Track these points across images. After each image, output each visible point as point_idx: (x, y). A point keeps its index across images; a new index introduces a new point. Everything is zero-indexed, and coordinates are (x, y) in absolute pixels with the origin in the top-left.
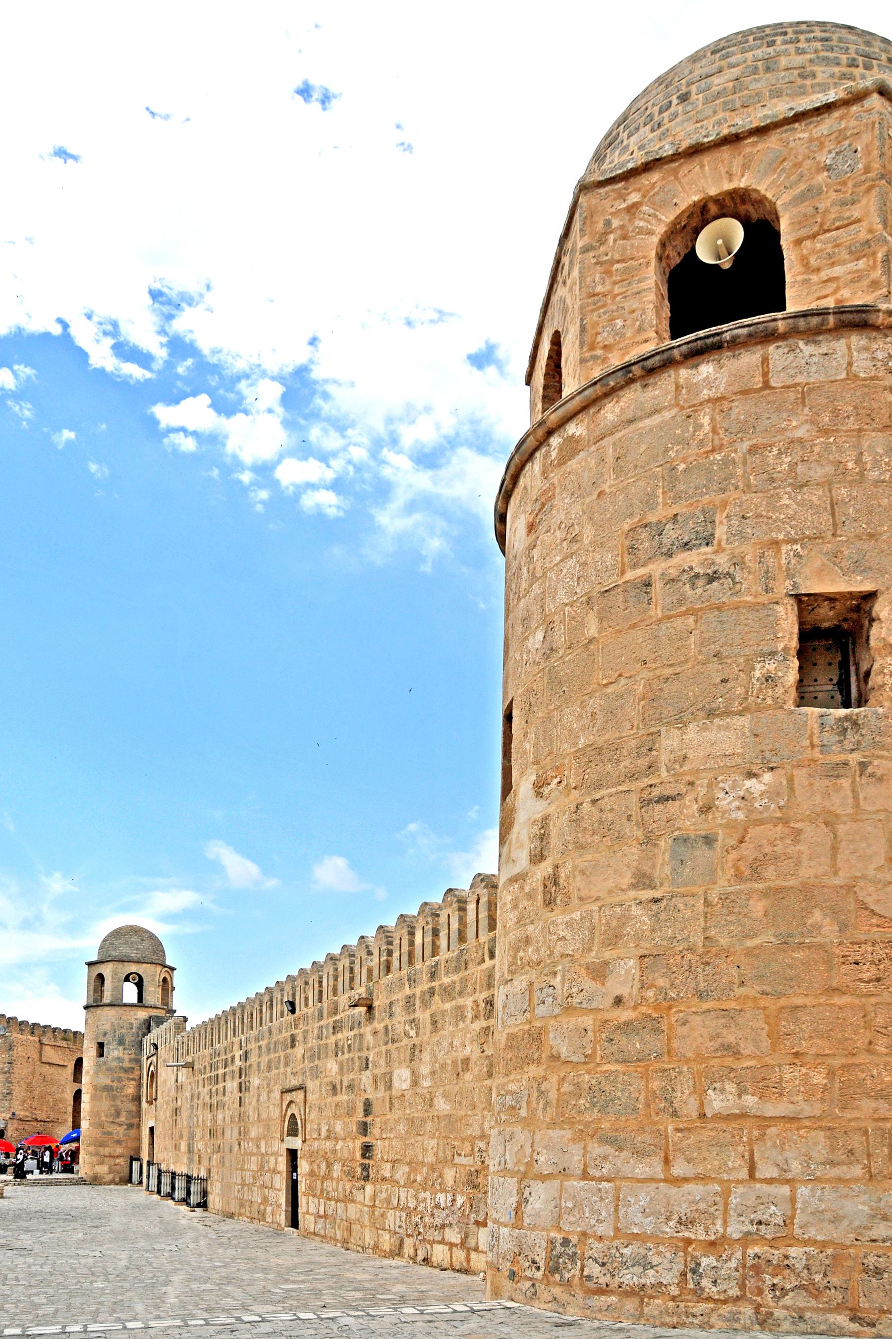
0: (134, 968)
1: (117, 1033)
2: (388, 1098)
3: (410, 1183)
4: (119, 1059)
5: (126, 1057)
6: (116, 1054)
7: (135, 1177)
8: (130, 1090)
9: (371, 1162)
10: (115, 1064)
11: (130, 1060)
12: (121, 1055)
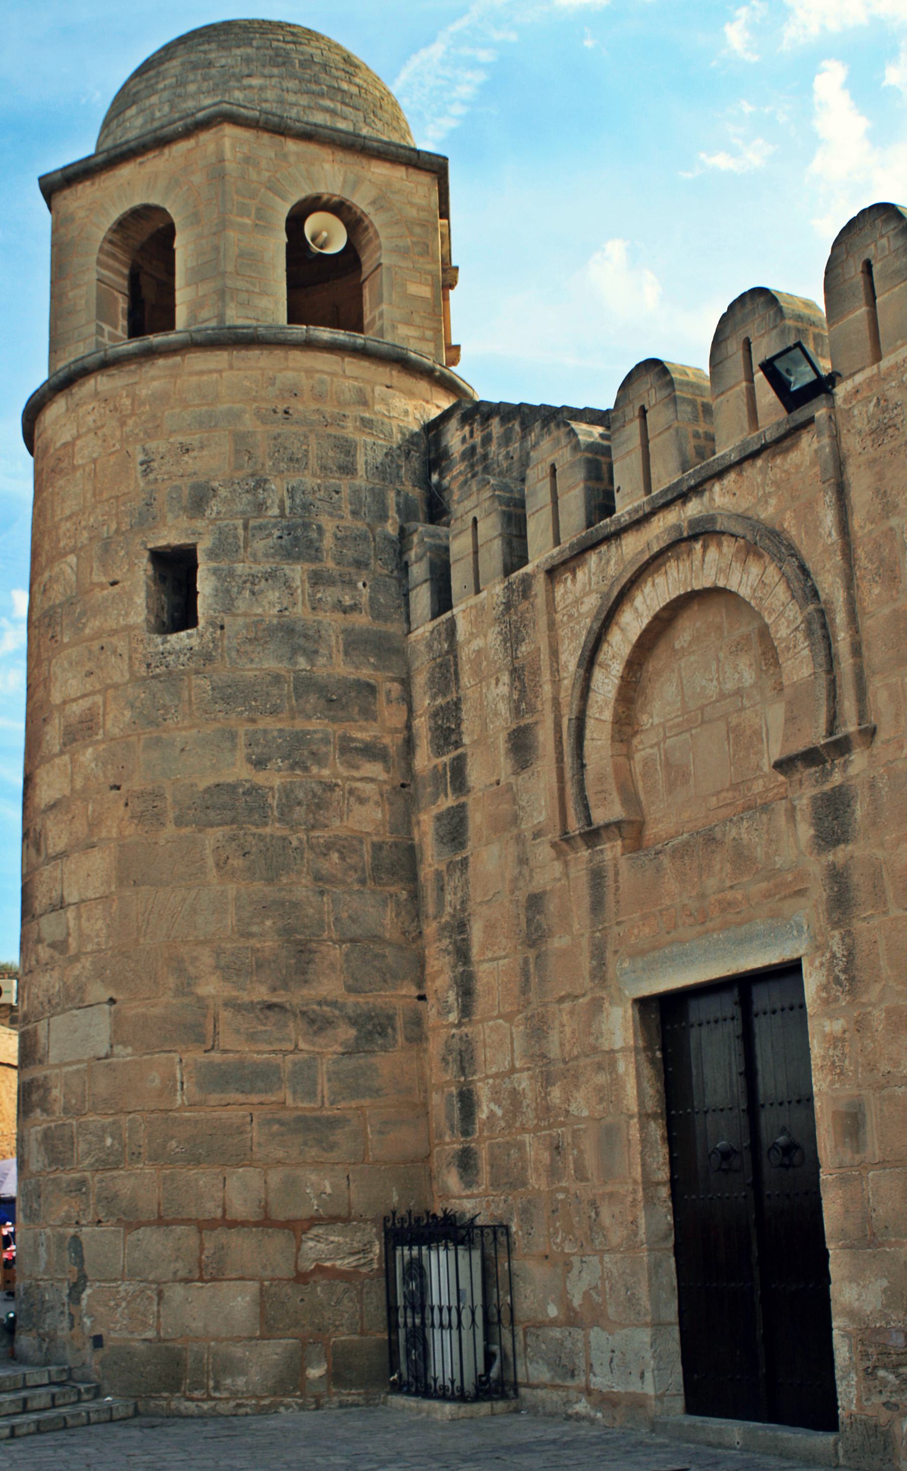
0: (330, 175)
1: (277, 488)
4: (292, 636)
5: (332, 622)
6: (269, 604)
10: (270, 662)
12: (300, 611)
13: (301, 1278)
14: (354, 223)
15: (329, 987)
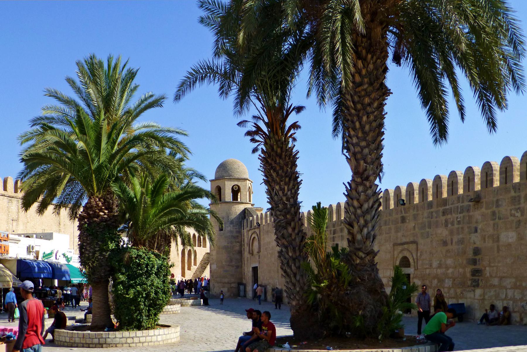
2: (496, 247)
3: (515, 287)
4: (231, 232)
5: (235, 230)
6: (229, 229)
7: (242, 293)
8: (237, 248)
9: (480, 278)
11: (237, 232)
13: (231, 288)
14: (238, 186)
15: (233, 263)
